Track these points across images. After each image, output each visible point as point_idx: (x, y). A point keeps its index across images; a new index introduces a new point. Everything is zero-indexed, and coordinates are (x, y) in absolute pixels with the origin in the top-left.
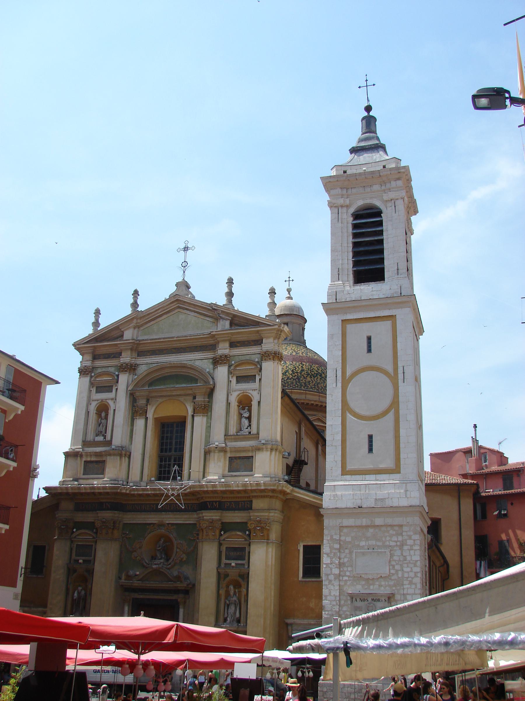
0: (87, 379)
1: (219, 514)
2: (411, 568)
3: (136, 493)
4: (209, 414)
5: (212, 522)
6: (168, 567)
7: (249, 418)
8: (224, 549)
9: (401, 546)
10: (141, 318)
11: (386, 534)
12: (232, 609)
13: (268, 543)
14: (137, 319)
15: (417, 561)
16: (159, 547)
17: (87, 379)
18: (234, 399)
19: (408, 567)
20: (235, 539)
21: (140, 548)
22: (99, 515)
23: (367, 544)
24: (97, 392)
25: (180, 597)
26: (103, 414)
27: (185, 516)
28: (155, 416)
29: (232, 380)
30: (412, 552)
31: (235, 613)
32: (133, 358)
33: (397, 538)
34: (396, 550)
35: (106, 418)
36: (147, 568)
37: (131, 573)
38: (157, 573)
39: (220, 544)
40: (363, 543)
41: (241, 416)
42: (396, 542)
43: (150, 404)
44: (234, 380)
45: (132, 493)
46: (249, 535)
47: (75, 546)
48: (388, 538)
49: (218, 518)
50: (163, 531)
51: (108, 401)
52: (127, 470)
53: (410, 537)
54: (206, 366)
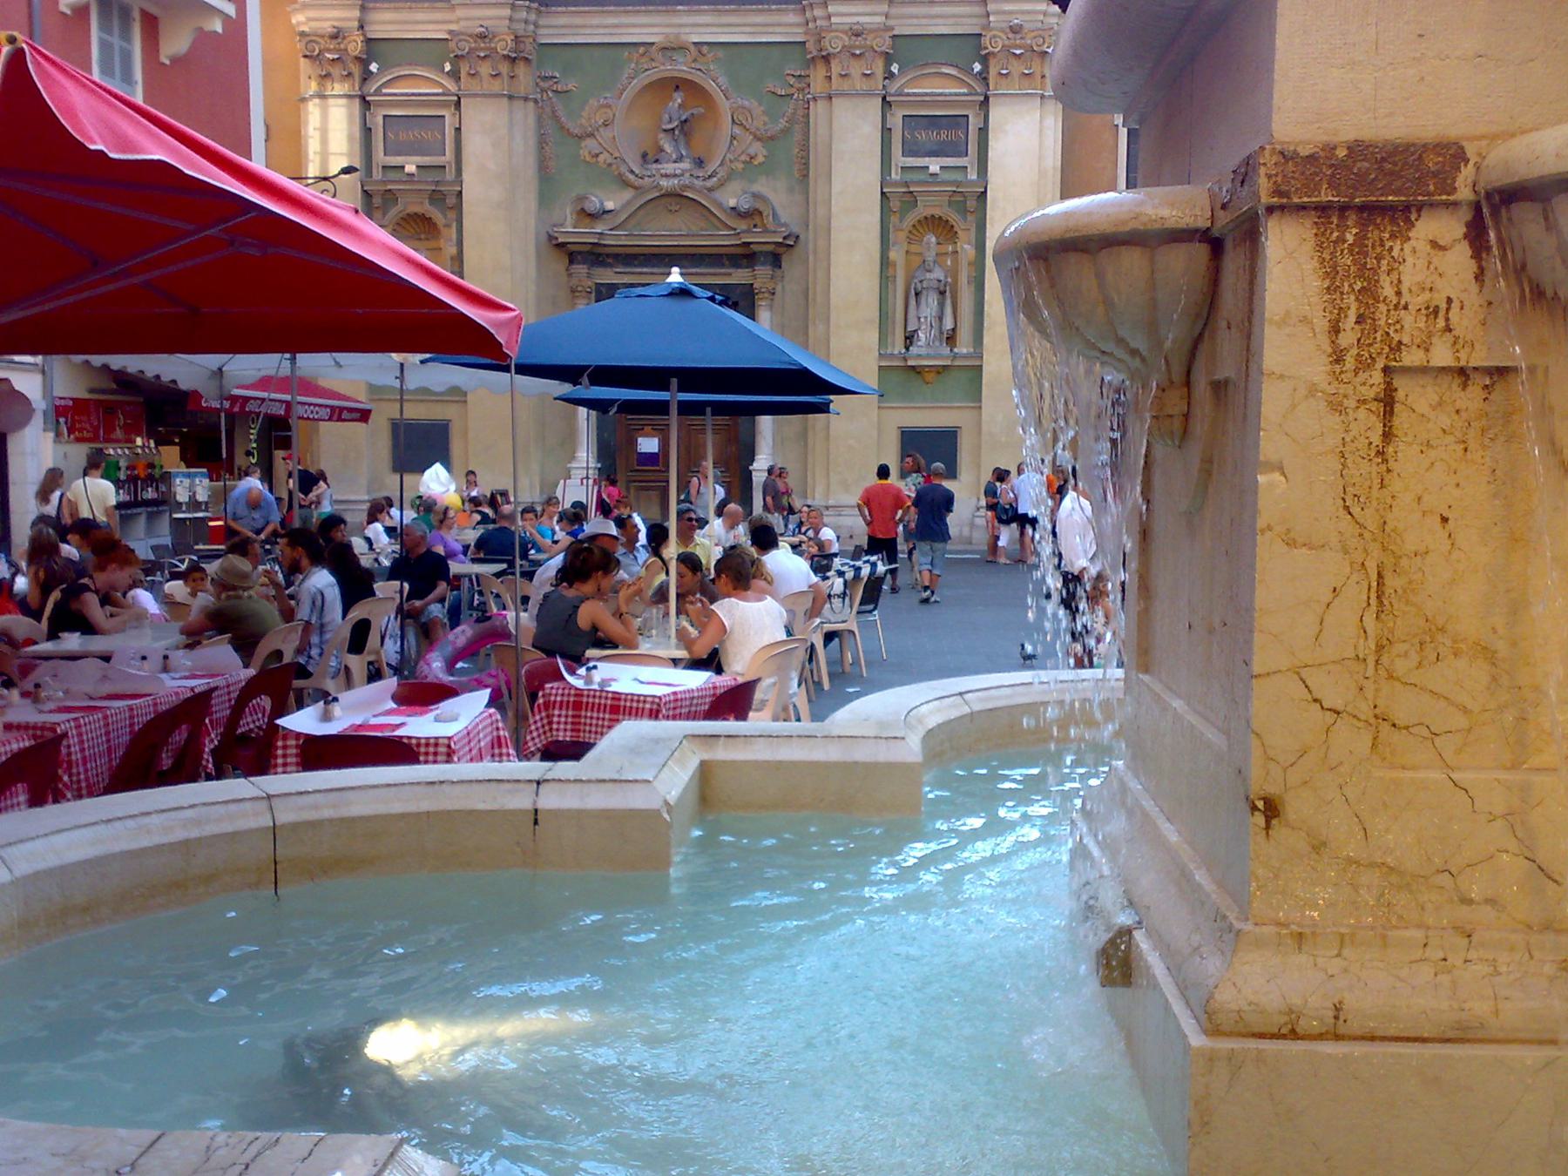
6: (709, 184)
8: (896, 121)
12: (930, 304)
13: (1042, 97)
20: (940, 88)
25: (760, 276)
27: (759, 19)
31: (941, 318)
36: (636, 188)
37: (593, 204)
38: (676, 198)
39: (886, 103)
46: (983, 77)
47: (380, 120)
49: (880, 19)
50: (681, 67)
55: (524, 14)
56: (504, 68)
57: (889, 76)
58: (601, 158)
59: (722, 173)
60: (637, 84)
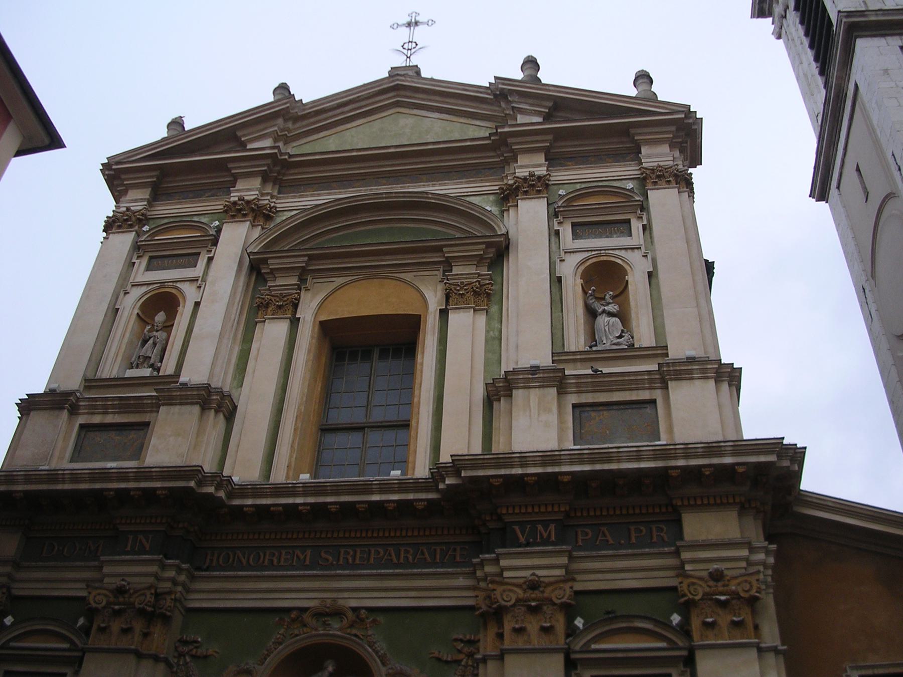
0: (125, 240)
1: (564, 560)
3: (249, 502)
4: (494, 309)
5: (534, 585)
10: (297, 119)
13: (760, 650)
14: (286, 120)
17: (125, 240)
18: (569, 269)
22: (106, 570)
24: (148, 269)
26: (160, 317)
28: (323, 318)
29: (561, 229)
32: (268, 194)
35: (168, 327)
43: (307, 290)
45: (237, 502)
46: (685, 630)
51: (178, 285)
52: (219, 453)
55: (171, 574)
56: (138, 626)
57: (571, 632)
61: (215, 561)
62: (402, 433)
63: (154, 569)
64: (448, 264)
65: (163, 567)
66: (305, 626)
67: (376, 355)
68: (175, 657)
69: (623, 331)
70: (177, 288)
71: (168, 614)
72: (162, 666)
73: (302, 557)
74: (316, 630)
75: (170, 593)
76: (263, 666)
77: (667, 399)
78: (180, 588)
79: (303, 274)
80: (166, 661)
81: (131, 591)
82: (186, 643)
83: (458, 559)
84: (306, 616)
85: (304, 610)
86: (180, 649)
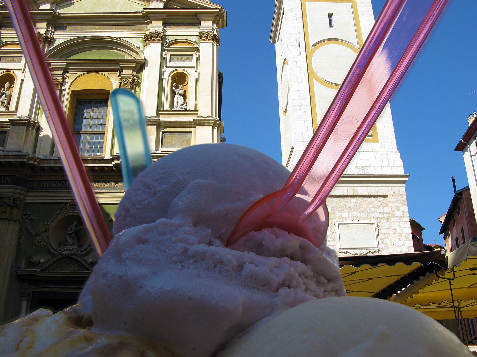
2: (403, 242)
3: (46, 165)
6: (83, 253)
7: (184, 96)
9: (388, 218)
11: (371, 205)
15: (408, 234)
16: (71, 230)
19: (399, 240)
21: (45, 231)
23: (350, 216)
28: (73, 89)
30: (402, 225)
33: (383, 209)
34: (383, 222)
36: (53, 254)
37: (35, 259)
40: (345, 215)
41: (173, 93)
42: (383, 213)
44: (168, 56)
45: (41, 165)
48: (373, 210)
53: (398, 209)
54: (137, 43)
55: (19, 191)
56: (8, 210)
58: (42, 243)
59: (88, 249)
60: (60, 217)
61: (34, 186)
62: (102, 135)
63: (12, 190)
64: (121, 69)
65: (16, 189)
66: (67, 209)
67: (94, 102)
68: (21, 219)
69: (184, 103)
70: (13, 72)
71: (19, 206)
72: (17, 223)
73: (65, 185)
74: (70, 210)
75: (19, 198)
76: (53, 223)
77: (195, 132)
78: (22, 196)
79: (65, 70)
80: (19, 222)
81: (5, 198)
82: (26, 215)
83: (119, 187)
84: (67, 206)
85: (67, 203)
86: (23, 217)
